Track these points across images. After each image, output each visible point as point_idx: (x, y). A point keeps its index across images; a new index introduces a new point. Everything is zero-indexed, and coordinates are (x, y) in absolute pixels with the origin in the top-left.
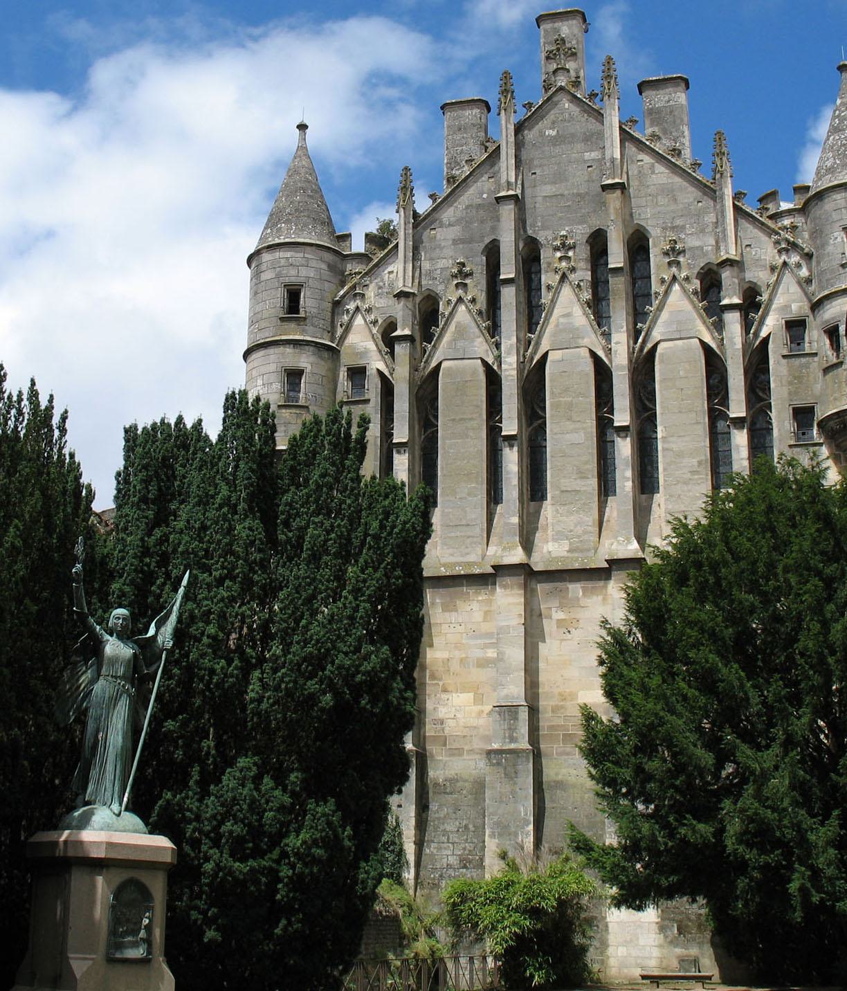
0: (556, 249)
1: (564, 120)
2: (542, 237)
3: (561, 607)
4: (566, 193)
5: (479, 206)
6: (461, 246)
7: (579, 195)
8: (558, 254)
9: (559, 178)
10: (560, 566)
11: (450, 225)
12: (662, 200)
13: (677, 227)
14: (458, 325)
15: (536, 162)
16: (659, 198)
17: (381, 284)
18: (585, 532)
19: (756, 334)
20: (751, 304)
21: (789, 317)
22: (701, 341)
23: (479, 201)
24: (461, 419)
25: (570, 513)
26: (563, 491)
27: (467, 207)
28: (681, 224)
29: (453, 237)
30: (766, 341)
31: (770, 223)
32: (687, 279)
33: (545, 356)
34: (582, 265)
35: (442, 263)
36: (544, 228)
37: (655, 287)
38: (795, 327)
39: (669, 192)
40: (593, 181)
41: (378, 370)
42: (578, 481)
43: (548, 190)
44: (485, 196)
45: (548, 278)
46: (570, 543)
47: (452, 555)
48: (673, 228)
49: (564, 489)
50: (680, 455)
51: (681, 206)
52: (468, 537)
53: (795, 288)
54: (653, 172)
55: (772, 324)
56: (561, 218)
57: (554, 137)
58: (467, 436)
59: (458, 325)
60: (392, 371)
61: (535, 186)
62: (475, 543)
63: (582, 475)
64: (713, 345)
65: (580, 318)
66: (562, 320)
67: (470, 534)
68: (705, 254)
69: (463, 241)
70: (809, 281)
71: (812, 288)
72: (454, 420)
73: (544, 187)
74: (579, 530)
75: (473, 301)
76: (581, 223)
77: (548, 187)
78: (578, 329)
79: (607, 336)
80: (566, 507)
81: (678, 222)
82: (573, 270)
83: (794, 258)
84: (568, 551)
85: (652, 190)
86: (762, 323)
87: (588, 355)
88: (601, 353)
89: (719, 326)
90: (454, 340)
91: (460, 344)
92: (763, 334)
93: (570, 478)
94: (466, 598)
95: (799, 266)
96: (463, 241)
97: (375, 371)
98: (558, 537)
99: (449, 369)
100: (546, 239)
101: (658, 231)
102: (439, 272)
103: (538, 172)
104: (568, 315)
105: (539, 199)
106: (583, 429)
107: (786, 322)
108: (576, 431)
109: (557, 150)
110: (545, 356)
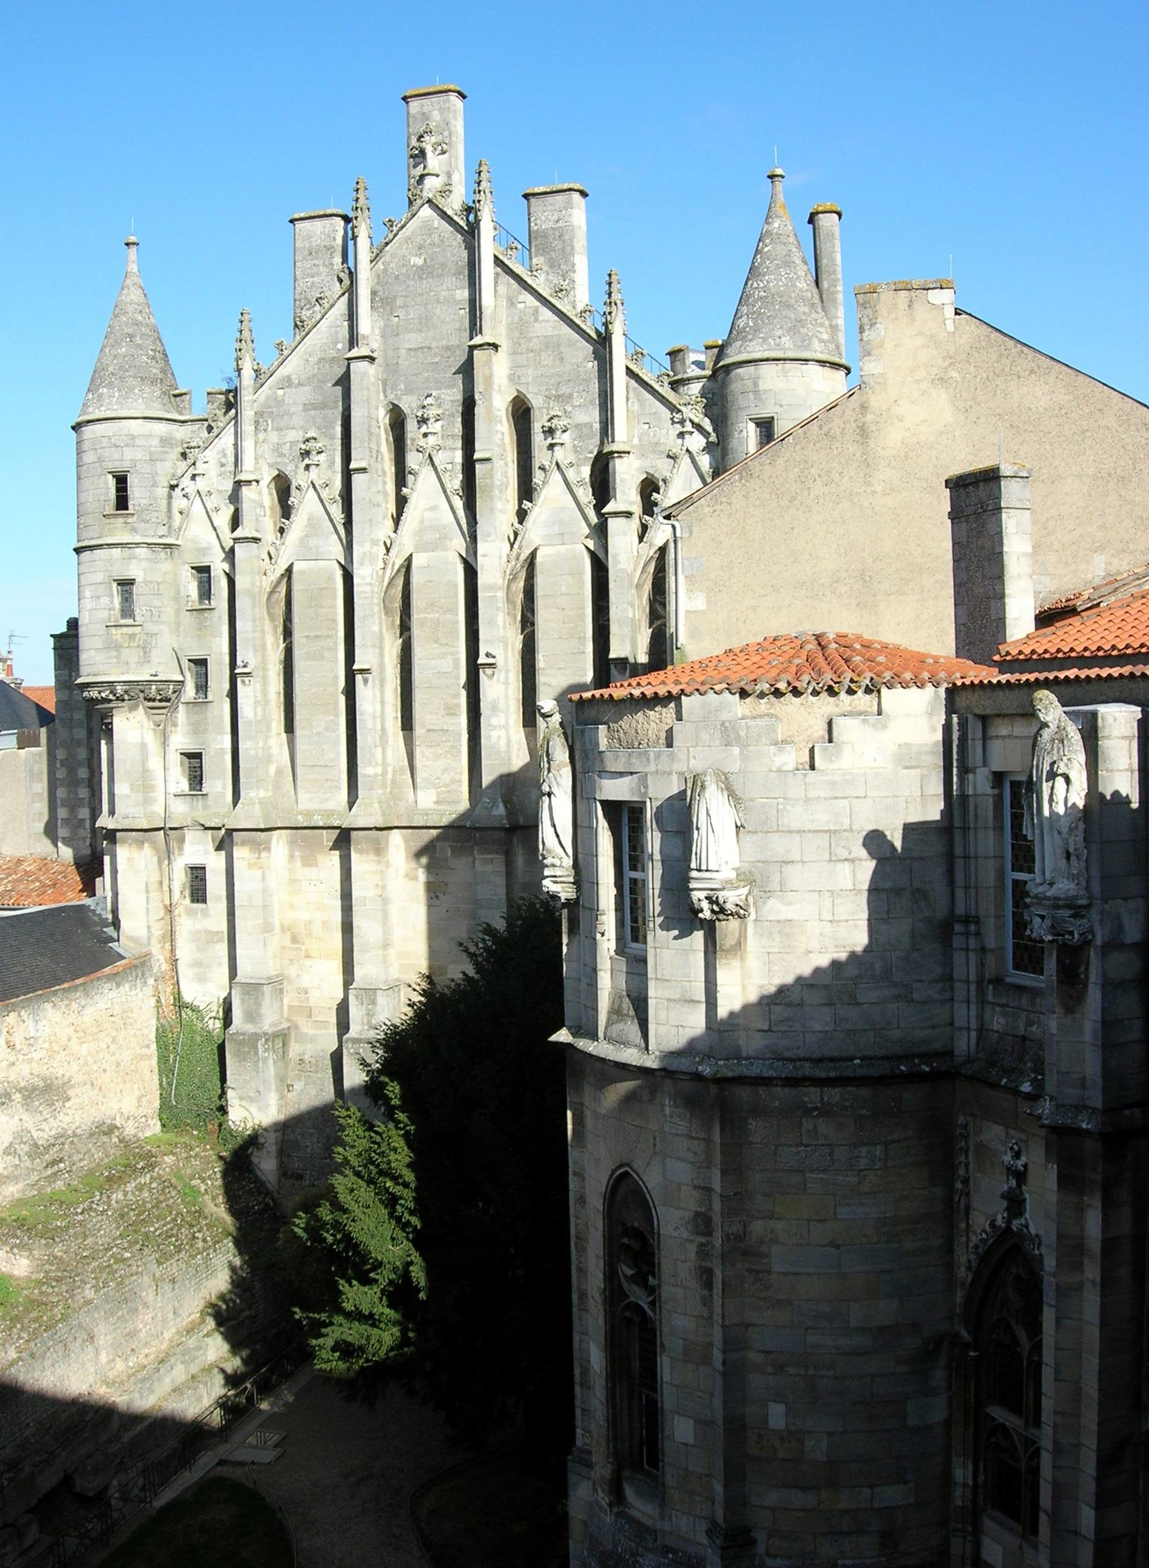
9: (425, 322)
12: (546, 359)
15: (399, 302)
16: (543, 354)
17: (223, 460)
24: (317, 636)
28: (568, 391)
33: (409, 560)
36: (408, 391)
39: (552, 345)
46: (438, 794)
48: (557, 397)
54: (536, 320)
56: (427, 379)
57: (421, 268)
61: (397, 335)
66: (427, 515)
72: (308, 637)
73: (408, 336)
74: (446, 778)
81: (564, 390)
85: (535, 344)
90: (307, 536)
91: (312, 542)
99: (302, 572)
100: (410, 407)
101: (541, 401)
102: (288, 446)
104: (433, 508)
105: (403, 352)
106: (451, 654)
110: (409, 560)
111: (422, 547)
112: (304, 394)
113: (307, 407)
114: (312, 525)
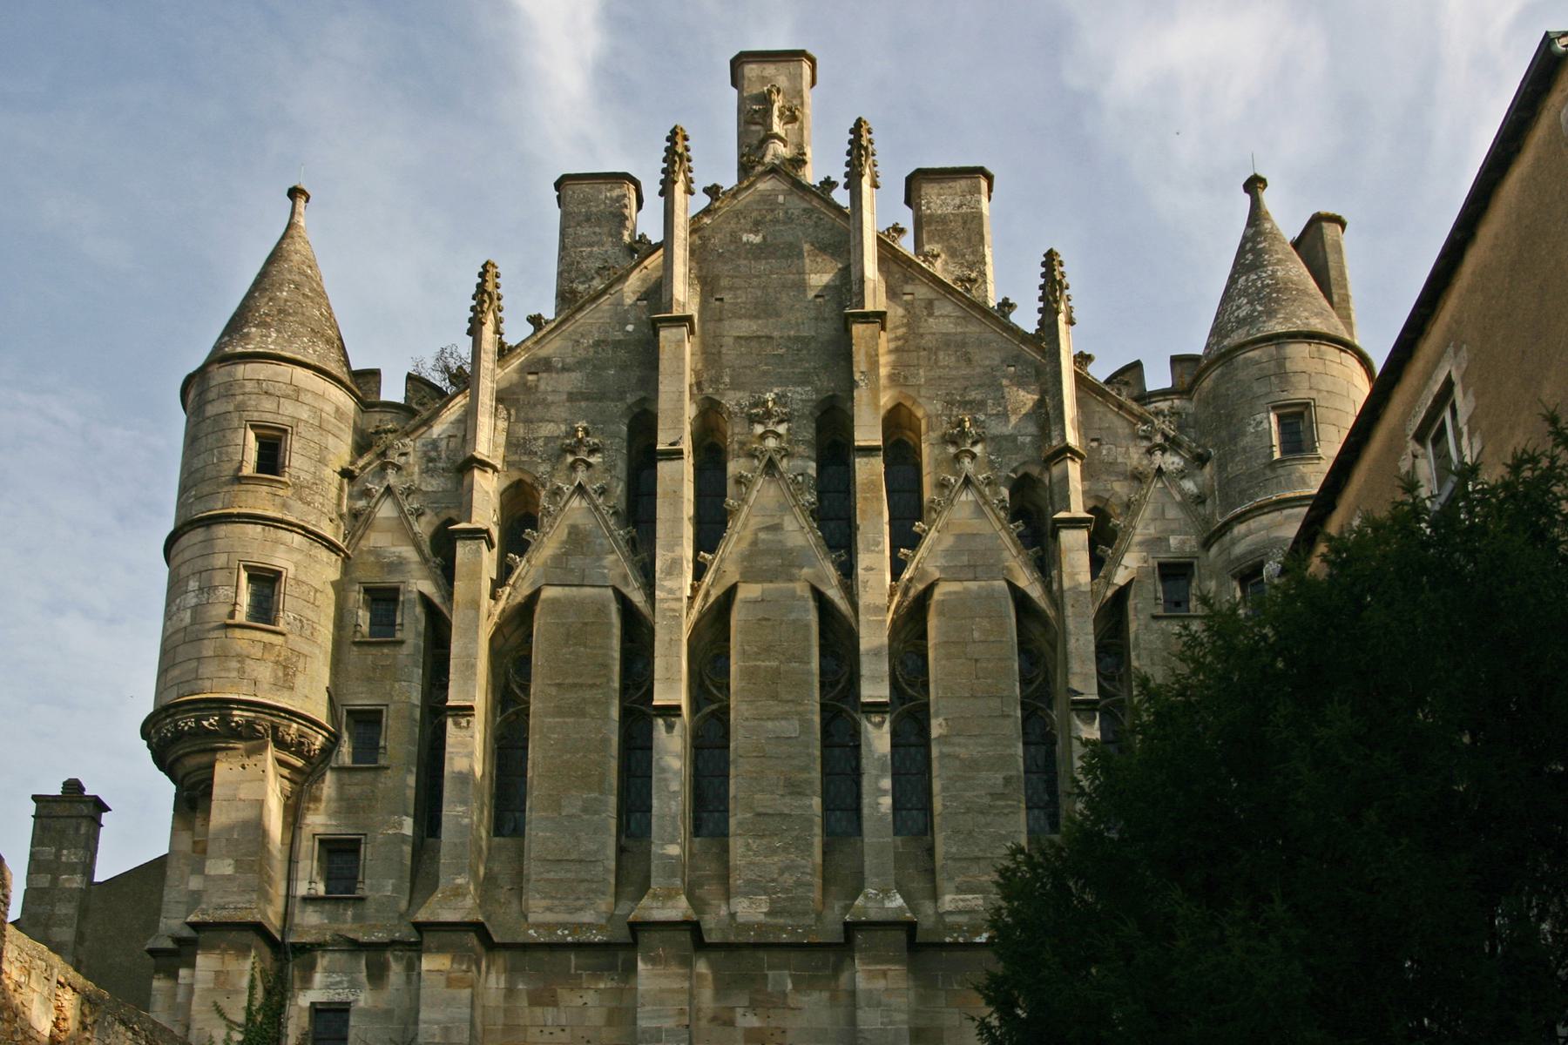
0: (753, 420)
1: (776, 221)
2: (731, 400)
3: (753, 1006)
4: (776, 334)
5: (617, 344)
6: (583, 404)
7: (797, 339)
8: (759, 429)
9: (764, 309)
10: (752, 936)
11: (565, 369)
13: (971, 402)
14: (574, 531)
15: (724, 282)
16: (941, 355)
17: (433, 454)
18: (799, 884)
19: (1109, 583)
20: (1104, 535)
21: (1163, 556)
22: (1013, 588)
23: (619, 336)
24: (575, 685)
25: (774, 851)
26: (759, 815)
27: (597, 344)
28: (979, 397)
29: (569, 388)
30: (1122, 593)
31: (1135, 406)
32: (989, 482)
34: (801, 449)
35: (547, 429)
36: (736, 385)
37: (928, 493)
38: (1174, 573)
39: (957, 345)
40: (825, 320)
41: (421, 594)
42: (787, 800)
43: (746, 327)
44: (630, 328)
45: (734, 467)
46: (772, 902)
47: (549, 909)
49: (761, 810)
50: (973, 765)
51: (978, 370)
52: (582, 881)
53: (1172, 513)
54: (930, 315)
55: (1130, 565)
56: (765, 373)
57: (757, 245)
58: (583, 714)
59: (574, 531)
60: (449, 596)
61: (720, 320)
62: (594, 891)
63: (795, 789)
64: (1035, 592)
65: (799, 533)
66: (762, 536)
67: (583, 875)
68: (1020, 448)
69: (587, 397)
70: (1200, 499)
71: (1207, 509)
72: (559, 685)
73: (738, 322)
74: (789, 879)
75: (603, 491)
76: (802, 383)
77: (745, 323)
78: (791, 551)
79: (847, 570)
80: (764, 841)
81: (973, 395)
82: (788, 455)
83: (1172, 462)
84: (766, 914)
85: (927, 341)
86: (1117, 563)
87: (808, 594)
88: (834, 593)
89: (1045, 562)
90: (566, 554)
91: (575, 562)
92: (1120, 578)
93: (772, 793)
94: (574, 983)
95: (1182, 474)
96: (587, 397)
97: (415, 596)
98: (754, 888)
99: (554, 601)
100: (738, 404)
101: (939, 407)
102: (541, 442)
103: (728, 297)
105: (728, 341)
106: (798, 713)
107: (1160, 565)
108: (785, 716)
109: (762, 266)
110: (730, 593)
111: (750, 575)
112: (572, 381)
113: (572, 397)
114: (577, 540)
